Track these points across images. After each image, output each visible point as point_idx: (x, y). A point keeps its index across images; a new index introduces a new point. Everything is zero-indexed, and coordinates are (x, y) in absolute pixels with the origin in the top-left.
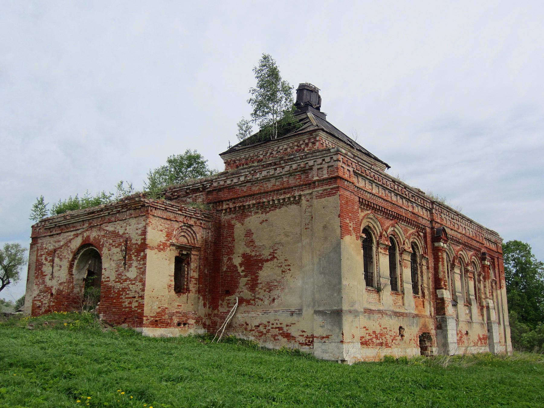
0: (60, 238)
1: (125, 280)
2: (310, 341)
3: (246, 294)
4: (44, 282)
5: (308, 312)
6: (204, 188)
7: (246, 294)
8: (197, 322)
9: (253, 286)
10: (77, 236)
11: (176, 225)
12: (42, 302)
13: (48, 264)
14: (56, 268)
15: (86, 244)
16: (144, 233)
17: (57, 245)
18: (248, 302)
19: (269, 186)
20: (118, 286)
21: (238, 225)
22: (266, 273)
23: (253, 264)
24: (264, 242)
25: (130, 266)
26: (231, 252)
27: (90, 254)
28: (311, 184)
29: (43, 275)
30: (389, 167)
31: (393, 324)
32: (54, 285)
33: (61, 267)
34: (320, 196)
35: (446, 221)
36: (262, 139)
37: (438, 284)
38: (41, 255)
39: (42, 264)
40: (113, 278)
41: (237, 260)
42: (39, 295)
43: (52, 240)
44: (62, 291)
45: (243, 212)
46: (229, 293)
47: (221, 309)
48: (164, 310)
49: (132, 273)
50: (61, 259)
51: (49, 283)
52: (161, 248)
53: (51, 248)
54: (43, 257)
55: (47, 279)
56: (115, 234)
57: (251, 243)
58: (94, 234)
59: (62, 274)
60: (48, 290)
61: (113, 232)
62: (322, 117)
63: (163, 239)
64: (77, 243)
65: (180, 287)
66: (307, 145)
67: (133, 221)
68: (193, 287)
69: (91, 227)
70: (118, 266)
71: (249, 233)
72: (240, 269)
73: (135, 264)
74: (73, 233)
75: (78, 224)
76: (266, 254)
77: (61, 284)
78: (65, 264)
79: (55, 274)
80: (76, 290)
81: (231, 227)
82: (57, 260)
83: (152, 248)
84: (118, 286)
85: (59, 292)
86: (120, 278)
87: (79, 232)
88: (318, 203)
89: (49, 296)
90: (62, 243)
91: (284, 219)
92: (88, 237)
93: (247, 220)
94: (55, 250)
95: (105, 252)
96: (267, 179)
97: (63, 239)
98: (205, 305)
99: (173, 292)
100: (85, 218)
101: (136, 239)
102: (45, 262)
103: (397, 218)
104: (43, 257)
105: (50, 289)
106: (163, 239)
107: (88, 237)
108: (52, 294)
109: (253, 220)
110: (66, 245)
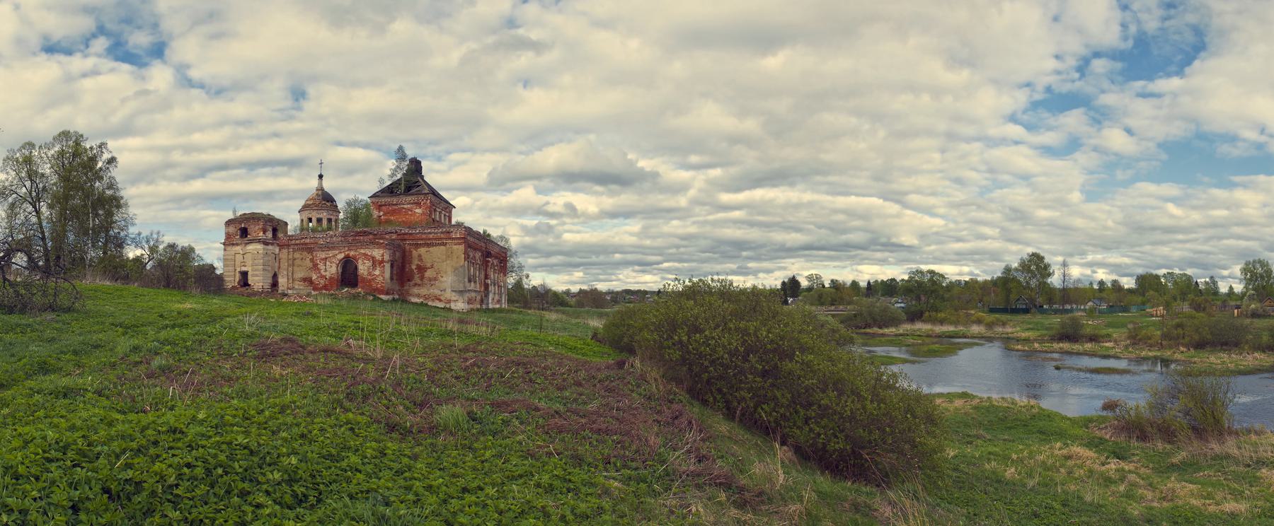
2: (449, 301)
3: (419, 282)
5: (449, 291)
7: (419, 282)
9: (422, 278)
15: (347, 257)
22: (428, 274)
23: (422, 269)
24: (428, 262)
26: (411, 263)
32: (328, 275)
35: (490, 247)
37: (486, 277)
41: (414, 267)
45: (417, 246)
49: (377, 272)
57: (421, 260)
58: (352, 253)
59: (334, 270)
60: (324, 277)
62: (422, 177)
64: (342, 256)
65: (392, 279)
71: (420, 256)
86: (370, 274)
88: (455, 247)
91: (438, 251)
97: (331, 253)
101: (378, 257)
103: (475, 249)
109: (422, 250)
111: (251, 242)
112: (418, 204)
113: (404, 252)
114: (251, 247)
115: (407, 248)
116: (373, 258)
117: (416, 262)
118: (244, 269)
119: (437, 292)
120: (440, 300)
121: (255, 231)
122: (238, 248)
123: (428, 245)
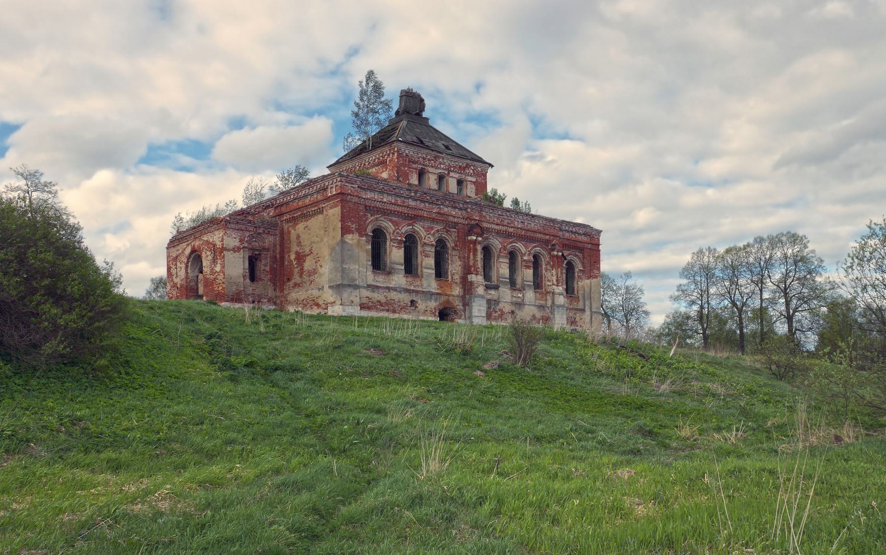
0: (179, 247)
6: (273, 205)
8: (269, 301)
10: (188, 245)
11: (247, 234)
15: (193, 251)
16: (222, 241)
18: (299, 285)
19: (307, 201)
21: (293, 231)
22: (308, 264)
26: (289, 252)
27: (196, 257)
28: (328, 199)
30: (491, 166)
31: (406, 298)
34: (331, 208)
36: (361, 150)
41: (293, 257)
45: (294, 220)
46: (289, 280)
47: (286, 292)
48: (240, 292)
52: (236, 250)
53: (175, 255)
56: (208, 242)
57: (299, 244)
58: (197, 243)
59: (182, 273)
61: (207, 241)
63: (237, 244)
64: (188, 251)
66: (389, 155)
67: (216, 233)
68: (266, 278)
69: (195, 238)
72: (294, 263)
73: (219, 261)
76: (307, 250)
78: (183, 266)
80: (192, 284)
81: (289, 232)
83: (229, 250)
85: (182, 285)
86: (213, 272)
93: (297, 227)
95: (204, 255)
96: (305, 196)
98: (275, 290)
99: (248, 281)
100: (191, 232)
101: (219, 244)
105: (176, 284)
106: (237, 244)
109: (301, 226)
110: (183, 252)
112: (382, 163)
113: (282, 234)
115: (286, 226)
116: (214, 245)
117: (295, 248)
119: (315, 293)
120: (318, 305)
123: (306, 217)
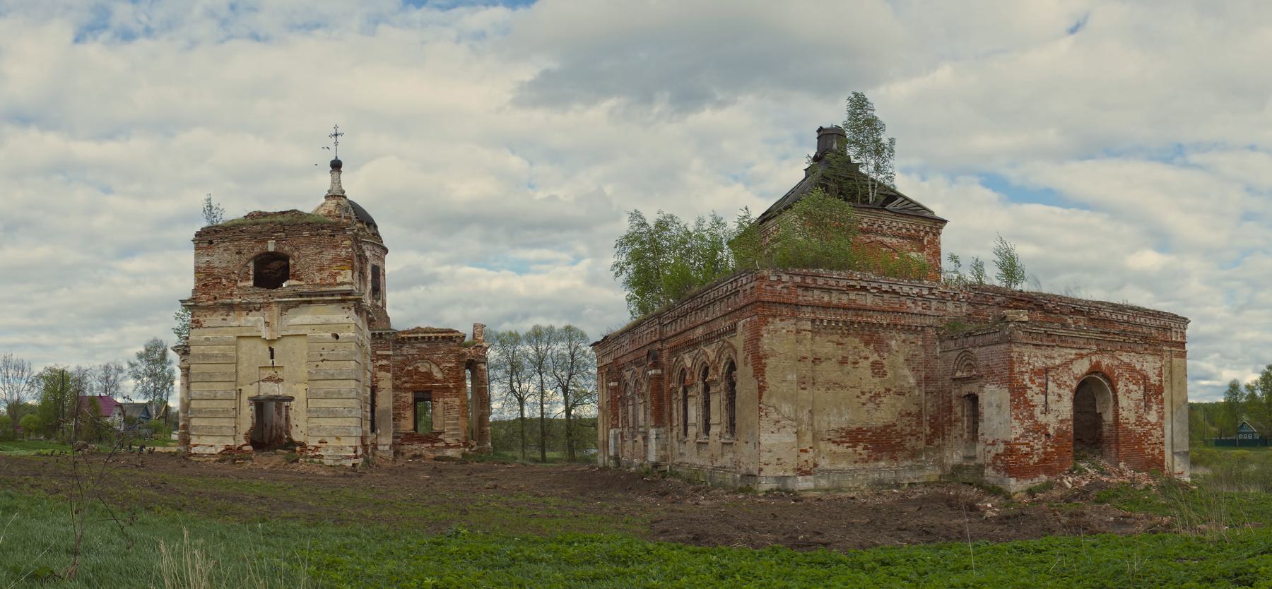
0: (1055, 353)
1: (1146, 424)
4: (1031, 416)
10: (1082, 356)
12: (1032, 447)
13: (1036, 389)
14: (1050, 398)
15: (1095, 369)
17: (1049, 363)
20: (1139, 430)
25: (1150, 409)
29: (1029, 405)
33: (1060, 396)
38: (1022, 373)
39: (1025, 388)
40: (1133, 420)
42: (1022, 436)
43: (1039, 352)
44: (1066, 432)
49: (1153, 417)
50: (1059, 386)
51: (1042, 419)
54: (1026, 377)
55: (1037, 411)
60: (1040, 429)
64: (1082, 367)
70: (1137, 406)
73: (1155, 407)
74: (1074, 352)
75: (1081, 342)
77: (1062, 421)
79: (1052, 406)
82: (1052, 386)
84: (1139, 430)
85: (1060, 434)
86: (1140, 421)
87: (1084, 352)
89: (1043, 439)
90: (1057, 362)
92: (1098, 363)
94: (1047, 370)
97: (1059, 356)
102: (1029, 385)
104: (1026, 377)
107: (1098, 363)
108: (1048, 435)
110: (1067, 365)
111: (308, 299)
114: (302, 319)
118: (270, 389)
121: (313, 263)
122: (254, 321)
